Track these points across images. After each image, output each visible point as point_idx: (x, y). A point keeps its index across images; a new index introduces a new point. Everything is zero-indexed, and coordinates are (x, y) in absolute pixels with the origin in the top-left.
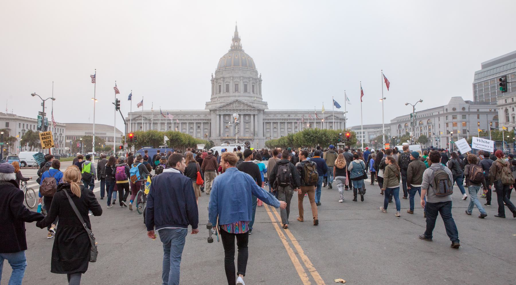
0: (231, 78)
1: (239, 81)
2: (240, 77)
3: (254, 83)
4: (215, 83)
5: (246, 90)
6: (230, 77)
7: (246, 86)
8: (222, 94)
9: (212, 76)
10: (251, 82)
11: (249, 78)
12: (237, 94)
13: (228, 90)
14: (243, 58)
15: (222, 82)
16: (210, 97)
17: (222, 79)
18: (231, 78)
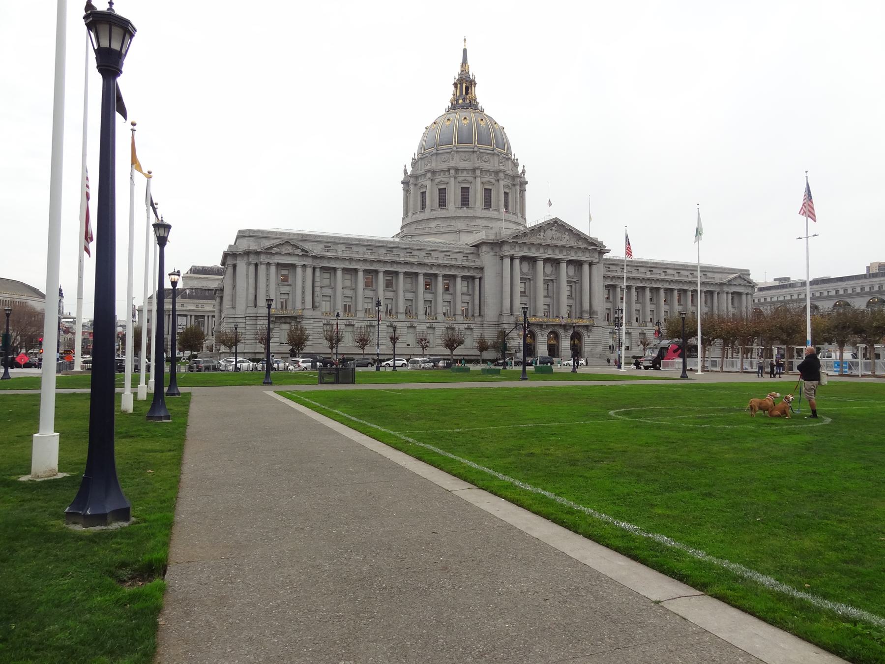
0: (452, 172)
1: (471, 179)
2: (474, 170)
3: (507, 186)
4: (412, 187)
5: (488, 203)
6: (449, 170)
7: (487, 192)
8: (427, 214)
9: (405, 172)
10: (502, 183)
11: (497, 173)
12: (464, 212)
13: (442, 203)
14: (483, 123)
15: (428, 183)
16: (400, 225)
17: (429, 175)
18: (452, 172)
